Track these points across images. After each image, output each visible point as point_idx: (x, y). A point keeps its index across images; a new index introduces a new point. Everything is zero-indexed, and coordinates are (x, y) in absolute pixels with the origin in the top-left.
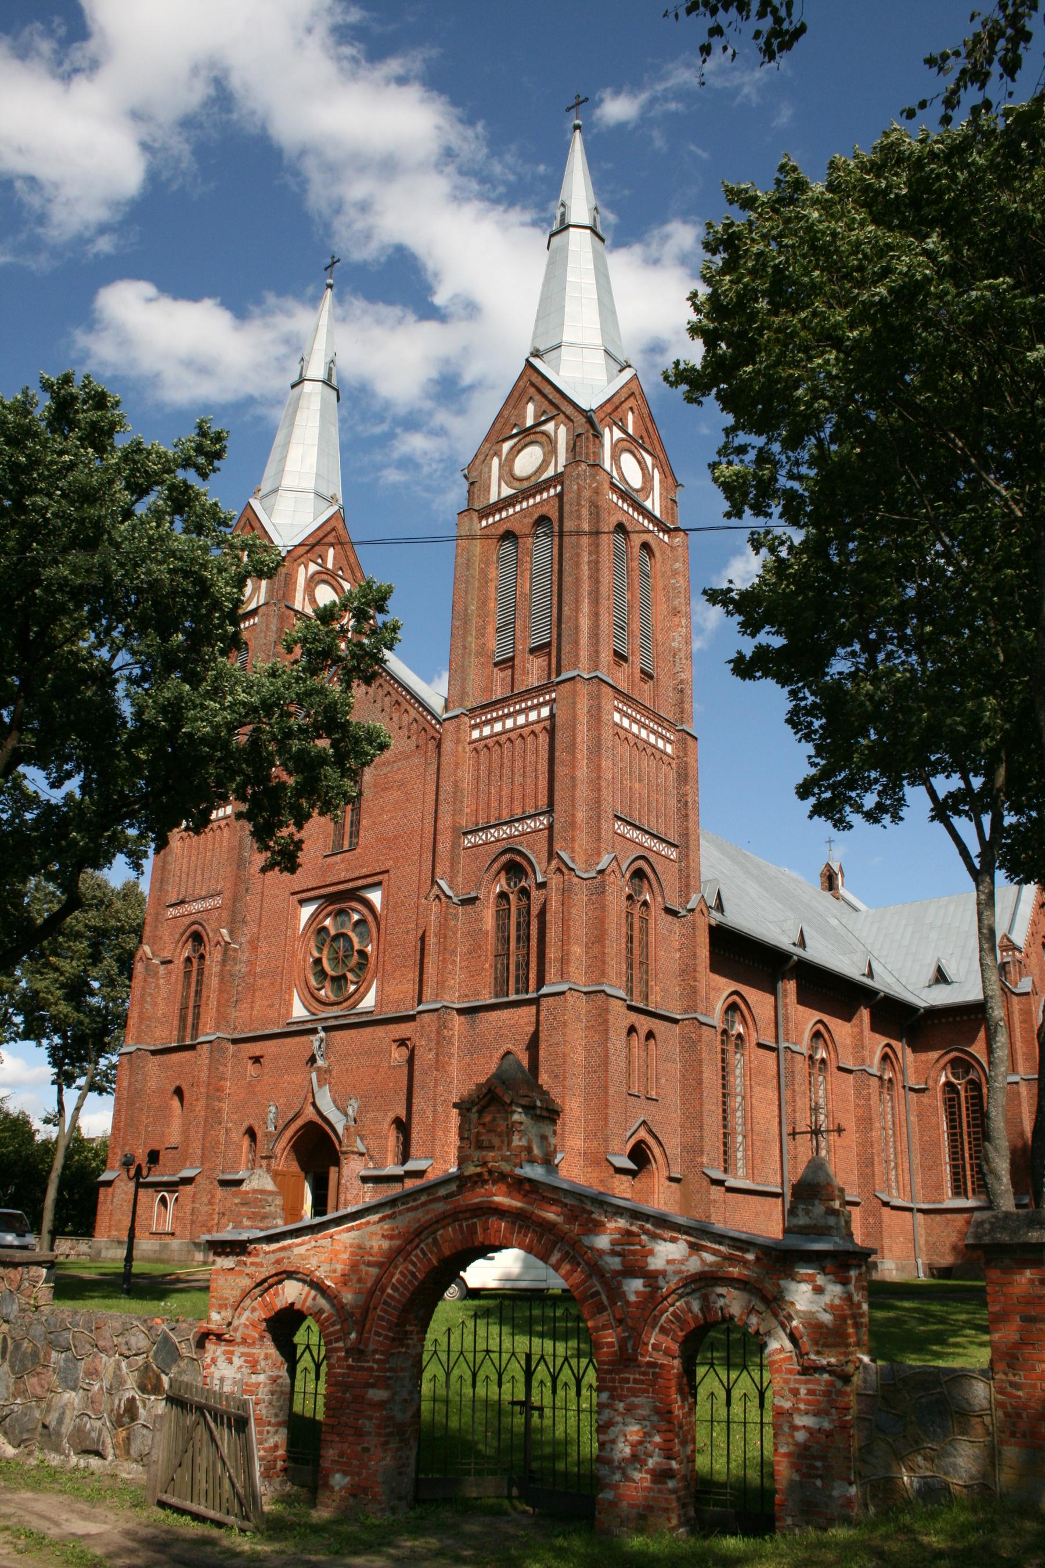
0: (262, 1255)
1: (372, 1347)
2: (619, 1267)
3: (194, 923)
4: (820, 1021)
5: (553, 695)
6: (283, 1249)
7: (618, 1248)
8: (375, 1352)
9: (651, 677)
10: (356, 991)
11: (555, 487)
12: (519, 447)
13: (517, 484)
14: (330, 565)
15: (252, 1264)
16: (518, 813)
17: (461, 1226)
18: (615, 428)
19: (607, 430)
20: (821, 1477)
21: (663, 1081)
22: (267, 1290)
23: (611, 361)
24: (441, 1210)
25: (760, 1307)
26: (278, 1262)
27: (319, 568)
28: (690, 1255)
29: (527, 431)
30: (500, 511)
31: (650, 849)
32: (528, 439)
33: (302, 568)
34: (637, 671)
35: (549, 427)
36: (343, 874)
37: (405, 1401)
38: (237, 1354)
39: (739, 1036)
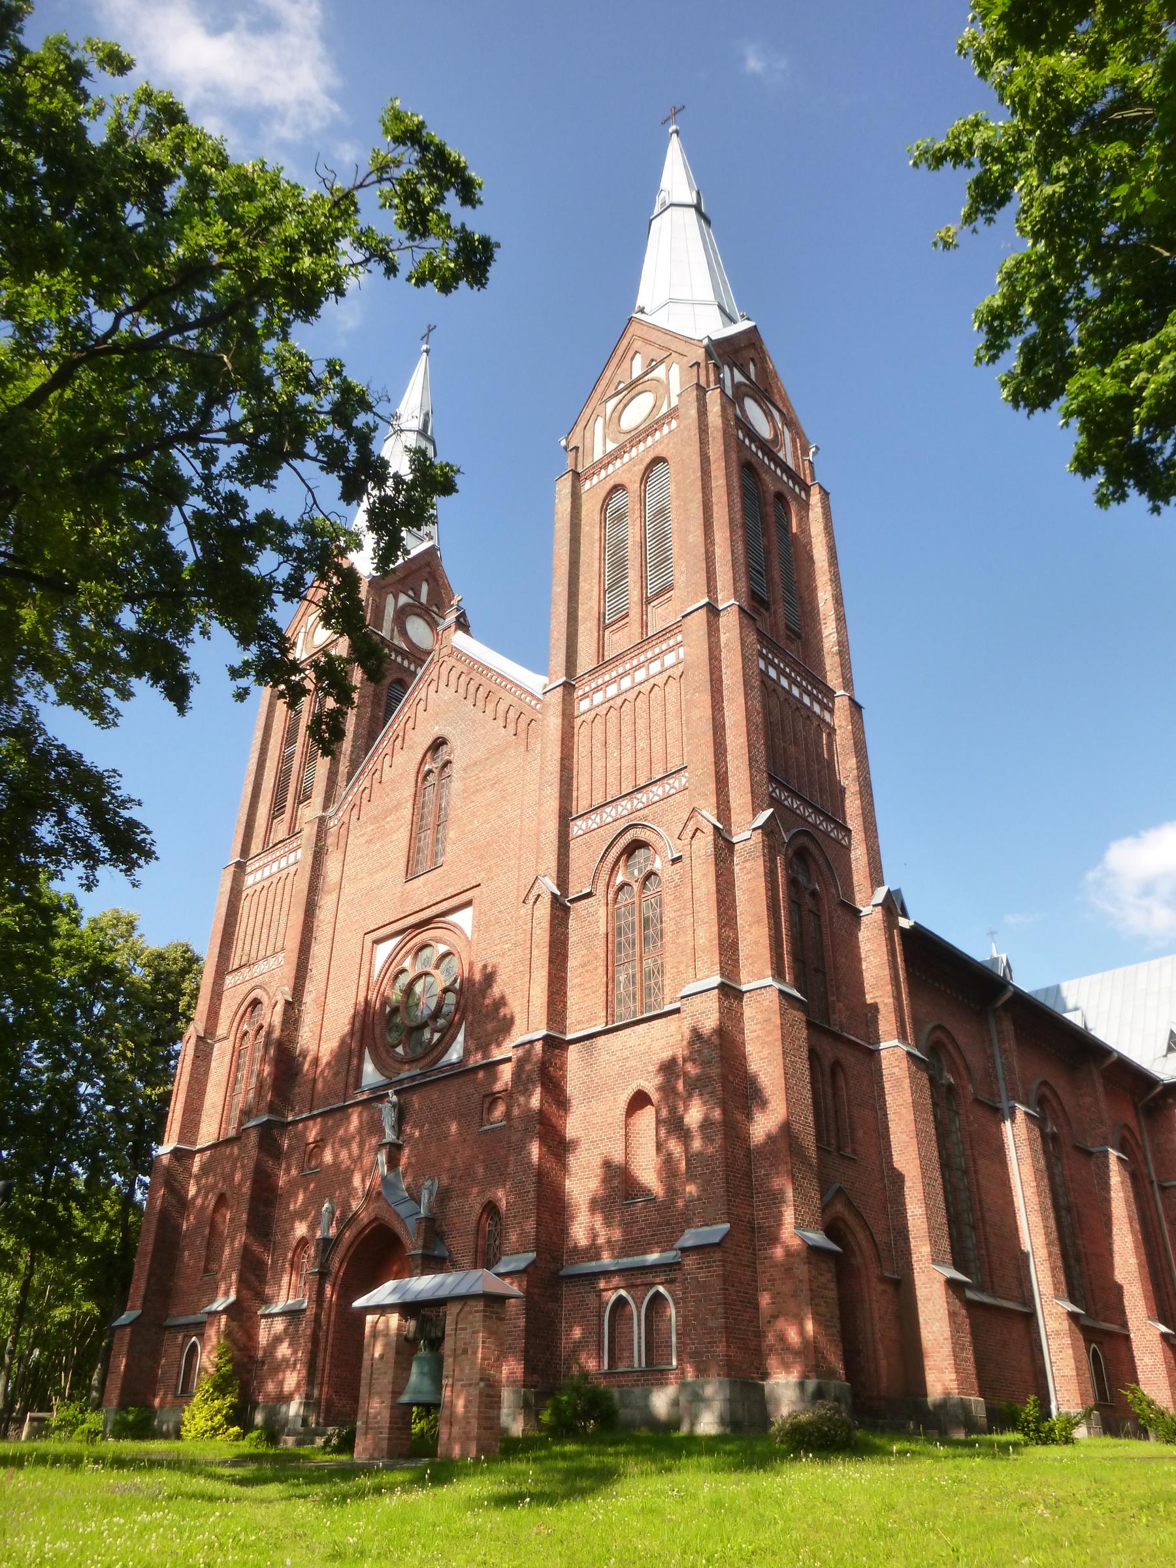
3: (253, 989)
5: (679, 638)
10: (440, 1040)
11: (669, 423)
12: (625, 401)
14: (424, 599)
16: (642, 782)
21: (860, 1133)
27: (411, 601)
29: (633, 384)
30: (605, 467)
31: (815, 826)
33: (390, 598)
35: (660, 372)
36: (425, 900)
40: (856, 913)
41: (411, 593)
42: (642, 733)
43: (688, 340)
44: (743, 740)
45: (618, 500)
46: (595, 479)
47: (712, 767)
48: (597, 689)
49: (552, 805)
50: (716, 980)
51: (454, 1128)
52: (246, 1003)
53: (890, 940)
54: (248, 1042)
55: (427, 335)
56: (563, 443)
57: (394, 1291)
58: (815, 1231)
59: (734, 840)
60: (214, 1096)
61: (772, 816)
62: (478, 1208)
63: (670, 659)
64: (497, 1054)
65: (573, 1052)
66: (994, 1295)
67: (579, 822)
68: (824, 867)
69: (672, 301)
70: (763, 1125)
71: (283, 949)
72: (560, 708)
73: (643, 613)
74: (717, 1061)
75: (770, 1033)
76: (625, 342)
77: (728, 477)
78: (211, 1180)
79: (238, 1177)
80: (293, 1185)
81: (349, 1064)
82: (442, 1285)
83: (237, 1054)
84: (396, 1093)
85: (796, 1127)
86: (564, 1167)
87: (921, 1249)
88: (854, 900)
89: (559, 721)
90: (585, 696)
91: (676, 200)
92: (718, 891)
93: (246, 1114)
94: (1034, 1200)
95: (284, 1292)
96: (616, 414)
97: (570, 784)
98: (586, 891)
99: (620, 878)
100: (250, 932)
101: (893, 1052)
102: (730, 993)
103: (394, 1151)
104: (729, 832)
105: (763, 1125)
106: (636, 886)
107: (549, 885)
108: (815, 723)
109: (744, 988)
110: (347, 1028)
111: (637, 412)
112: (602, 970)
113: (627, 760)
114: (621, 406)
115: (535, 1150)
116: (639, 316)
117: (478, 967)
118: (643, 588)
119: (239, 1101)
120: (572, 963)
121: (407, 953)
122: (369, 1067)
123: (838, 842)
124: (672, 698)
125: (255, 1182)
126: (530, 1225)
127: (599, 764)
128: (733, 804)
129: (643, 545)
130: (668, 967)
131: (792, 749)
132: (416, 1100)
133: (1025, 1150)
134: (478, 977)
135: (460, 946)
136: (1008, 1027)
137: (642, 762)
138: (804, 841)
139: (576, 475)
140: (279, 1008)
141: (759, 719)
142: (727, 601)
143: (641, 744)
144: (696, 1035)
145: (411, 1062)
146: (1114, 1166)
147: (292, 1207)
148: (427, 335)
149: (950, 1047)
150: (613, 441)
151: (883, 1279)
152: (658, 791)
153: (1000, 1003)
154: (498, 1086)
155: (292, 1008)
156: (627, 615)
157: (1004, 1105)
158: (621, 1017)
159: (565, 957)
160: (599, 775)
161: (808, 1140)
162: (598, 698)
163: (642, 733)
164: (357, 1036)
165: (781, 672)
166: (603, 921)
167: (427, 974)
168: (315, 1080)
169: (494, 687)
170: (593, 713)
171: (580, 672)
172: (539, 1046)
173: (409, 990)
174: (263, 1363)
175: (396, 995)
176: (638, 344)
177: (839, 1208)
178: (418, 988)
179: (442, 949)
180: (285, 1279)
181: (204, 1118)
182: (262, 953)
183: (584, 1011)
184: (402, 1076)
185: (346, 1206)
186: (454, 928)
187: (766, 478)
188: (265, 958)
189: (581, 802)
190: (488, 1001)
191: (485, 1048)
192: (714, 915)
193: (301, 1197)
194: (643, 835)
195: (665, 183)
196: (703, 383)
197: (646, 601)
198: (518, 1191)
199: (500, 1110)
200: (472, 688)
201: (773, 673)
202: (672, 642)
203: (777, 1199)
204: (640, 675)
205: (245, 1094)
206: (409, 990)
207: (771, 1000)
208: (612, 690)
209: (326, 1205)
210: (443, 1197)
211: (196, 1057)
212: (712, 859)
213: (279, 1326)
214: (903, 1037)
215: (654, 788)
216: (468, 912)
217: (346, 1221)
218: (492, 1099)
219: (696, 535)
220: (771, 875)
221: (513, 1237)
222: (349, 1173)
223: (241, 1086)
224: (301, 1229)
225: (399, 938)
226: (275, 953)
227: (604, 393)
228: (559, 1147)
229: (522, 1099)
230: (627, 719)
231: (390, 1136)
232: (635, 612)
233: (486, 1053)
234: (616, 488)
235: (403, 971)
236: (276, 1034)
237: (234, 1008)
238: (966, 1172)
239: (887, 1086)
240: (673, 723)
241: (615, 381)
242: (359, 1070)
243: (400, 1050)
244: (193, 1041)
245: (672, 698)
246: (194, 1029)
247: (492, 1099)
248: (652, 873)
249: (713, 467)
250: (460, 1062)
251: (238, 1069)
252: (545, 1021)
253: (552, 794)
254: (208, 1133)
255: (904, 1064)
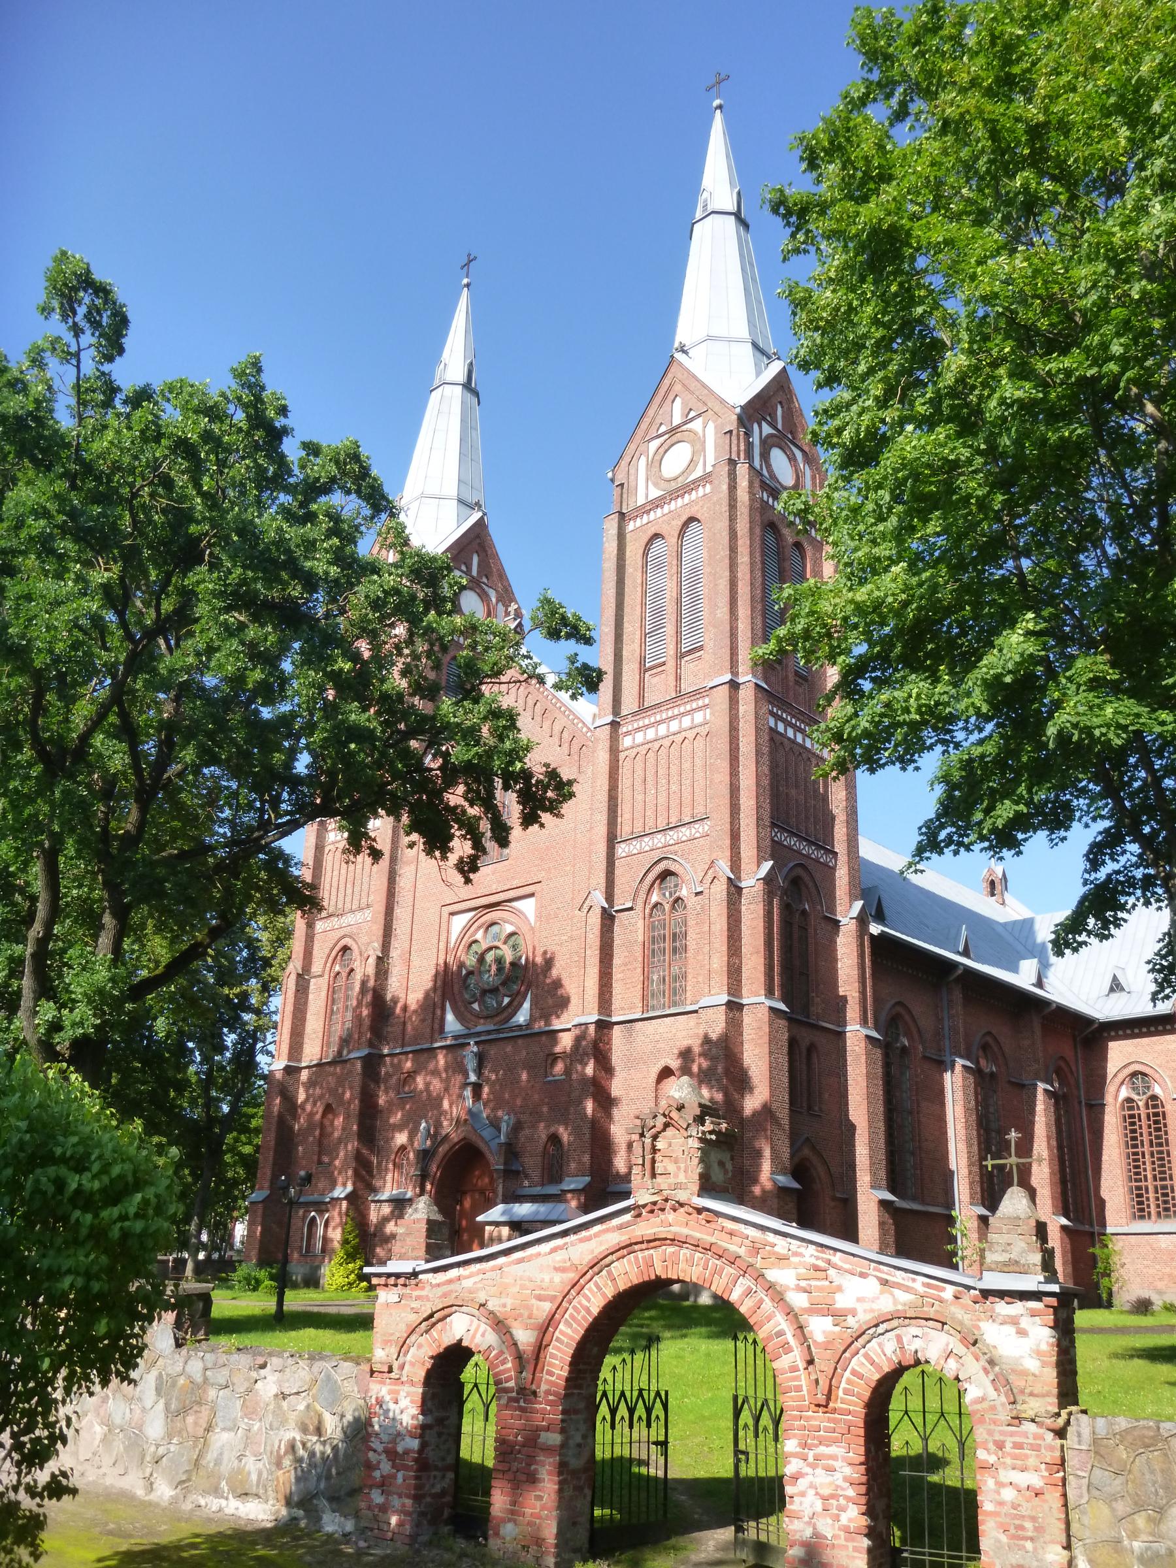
0: (428, 1288)
1: (544, 1387)
2: (806, 1305)
4: (989, 1033)
5: (707, 701)
6: (450, 1282)
7: (803, 1284)
8: (548, 1392)
9: (805, 679)
10: (510, 1004)
12: (665, 446)
13: (663, 484)
15: (418, 1298)
16: (674, 821)
17: (636, 1258)
18: (764, 424)
19: (756, 426)
20: (1032, 1539)
21: (826, 1096)
22: (434, 1325)
23: (758, 354)
24: (615, 1241)
25: (960, 1349)
26: (445, 1295)
28: (882, 1292)
29: (673, 431)
30: (648, 512)
31: (808, 856)
32: (674, 439)
34: (791, 677)
35: (696, 425)
37: (579, 1445)
38: (403, 1394)
39: (904, 1048)
40: (836, 923)
41: (464, 568)
42: (675, 778)
43: (722, 402)
44: (753, 802)
45: (658, 547)
46: (639, 522)
47: (728, 826)
48: (638, 729)
49: (602, 830)
50: (724, 998)
51: (524, 1076)
52: (337, 948)
53: (861, 945)
54: (341, 981)
55: (467, 264)
56: (610, 475)
57: (503, 1213)
58: (784, 1174)
59: (743, 885)
60: (314, 1024)
61: (772, 868)
62: (544, 1137)
63: (699, 717)
64: (557, 1025)
65: (617, 1031)
66: (923, 1203)
67: (623, 845)
68: (813, 890)
69: (710, 338)
70: (751, 1104)
71: (368, 906)
72: (607, 744)
73: (678, 667)
74: (720, 1062)
75: (761, 1037)
76: (667, 382)
77: (751, 554)
78: (318, 1091)
79: (348, 1095)
80: (390, 1103)
81: (434, 1013)
82: (537, 1212)
83: (332, 991)
84: (477, 1043)
85: (774, 1106)
86: (609, 1116)
87: (863, 1178)
88: (834, 912)
89: (607, 756)
90: (628, 733)
91: (717, 208)
92: (729, 929)
93: (345, 1042)
94: (962, 1132)
95: (389, 1185)
96: (658, 457)
97: (616, 812)
98: (629, 905)
99: (655, 898)
100: (335, 884)
101: (856, 1034)
102: (734, 1007)
103: (477, 1089)
104: (739, 878)
105: (751, 1104)
106: (667, 907)
107: (599, 898)
108: (814, 761)
109: (744, 1001)
110: (430, 985)
111: (676, 460)
112: (640, 970)
113: (662, 800)
114: (662, 450)
115: (589, 1106)
116: (679, 356)
117: (539, 952)
118: (678, 642)
119: (338, 1030)
120: (617, 961)
121: (479, 928)
122: (450, 1017)
123: (826, 865)
124: (699, 754)
125: (361, 1101)
126: (586, 1158)
127: (639, 797)
128: (743, 855)
129: (679, 601)
130: (689, 977)
131: (793, 792)
132: (493, 1051)
133: (959, 1095)
134: (539, 960)
135: (524, 929)
136: (957, 995)
137: (674, 804)
138: (800, 872)
139: (622, 515)
140: (372, 961)
141: (766, 782)
142: (746, 677)
143: (674, 788)
144: (707, 1040)
145: (486, 1018)
146: (1040, 1097)
147: (392, 1121)
148: (467, 264)
149: (907, 1017)
150: (656, 485)
151: (834, 1199)
152: (685, 833)
153: (952, 978)
154: (558, 1049)
155: (382, 962)
156: (664, 664)
157: (947, 1059)
158: (653, 1008)
159: (611, 956)
160: (639, 807)
161: (783, 1114)
162: (639, 737)
163: (675, 778)
164: (439, 992)
165: (788, 724)
166: (641, 931)
167: (497, 948)
168: (404, 1023)
169: (550, 707)
170: (635, 751)
171: (624, 712)
172: (592, 1028)
173: (481, 959)
174: (375, 1235)
175: (471, 961)
176: (678, 388)
177: (806, 1152)
178: (490, 957)
179: (509, 929)
180: (389, 1177)
181: (306, 1040)
182: (348, 906)
183: (626, 1001)
184: (479, 1028)
185: (438, 1125)
186: (518, 913)
187: (786, 531)
188: (352, 911)
189: (624, 830)
190: (548, 981)
191: (547, 1019)
192: (725, 948)
193: (399, 1115)
194: (673, 867)
195: (707, 181)
196: (734, 457)
197: (680, 656)
198: (576, 1132)
199: (559, 1067)
200: (530, 702)
201: (781, 727)
202: (700, 703)
203: (758, 1154)
204: (674, 726)
205: (343, 1023)
206: (481, 959)
207: (763, 1014)
208: (651, 734)
209: (423, 1125)
210: (517, 1128)
211: (297, 991)
212: (725, 904)
213: (386, 1209)
214: (864, 1022)
215: (683, 829)
216: (532, 900)
217: (436, 1138)
218: (554, 1058)
219: (723, 612)
220: (768, 915)
221: (573, 1165)
222: (440, 1099)
223: (338, 1017)
224: (401, 1138)
225: (472, 914)
226: (360, 909)
227: (648, 430)
228: (606, 1102)
229: (579, 1067)
230: (663, 762)
231: (473, 1078)
232: (671, 664)
233: (548, 1023)
234: (656, 536)
235: (476, 941)
236: (371, 983)
237: (327, 951)
238: (911, 1113)
239: (849, 1059)
240: (699, 775)
241: (658, 421)
242: (443, 1019)
243: (476, 1006)
244: (293, 977)
245: (699, 754)
246: (295, 966)
247: (554, 1058)
248: (679, 898)
249: (740, 542)
250: (528, 1025)
251: (333, 1003)
252: (596, 1005)
253: (602, 818)
254: (312, 1052)
255: (863, 1045)
